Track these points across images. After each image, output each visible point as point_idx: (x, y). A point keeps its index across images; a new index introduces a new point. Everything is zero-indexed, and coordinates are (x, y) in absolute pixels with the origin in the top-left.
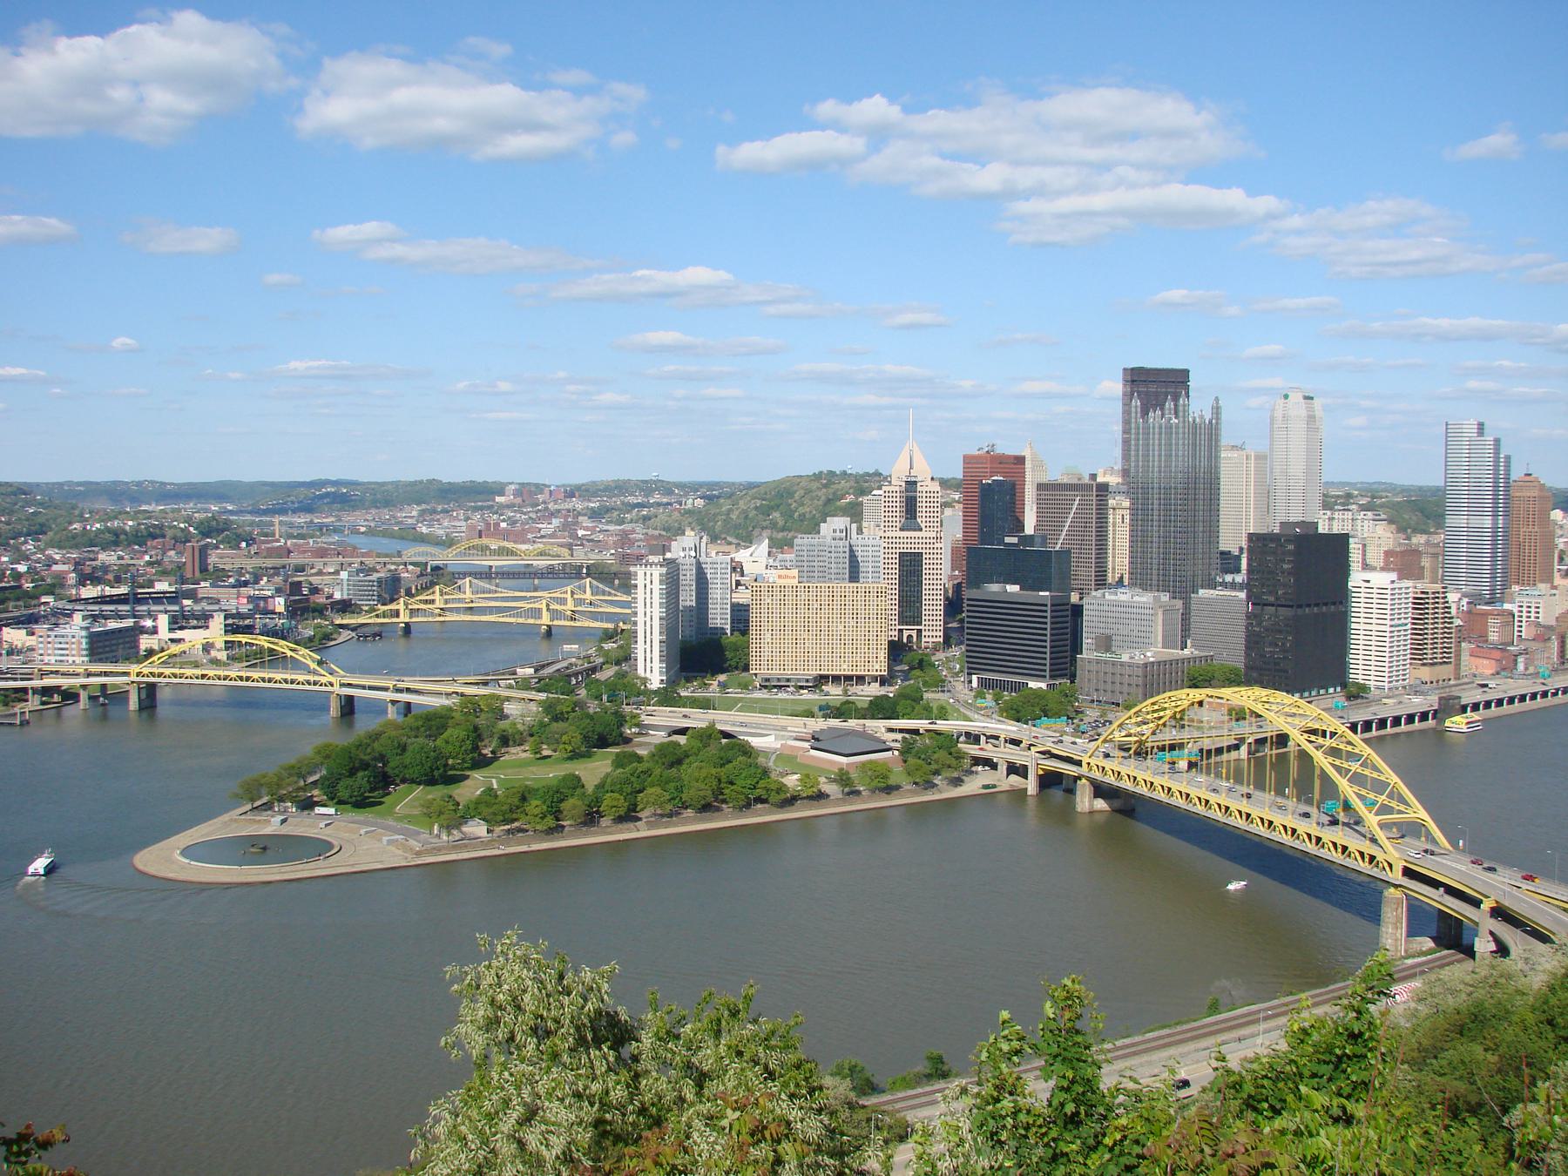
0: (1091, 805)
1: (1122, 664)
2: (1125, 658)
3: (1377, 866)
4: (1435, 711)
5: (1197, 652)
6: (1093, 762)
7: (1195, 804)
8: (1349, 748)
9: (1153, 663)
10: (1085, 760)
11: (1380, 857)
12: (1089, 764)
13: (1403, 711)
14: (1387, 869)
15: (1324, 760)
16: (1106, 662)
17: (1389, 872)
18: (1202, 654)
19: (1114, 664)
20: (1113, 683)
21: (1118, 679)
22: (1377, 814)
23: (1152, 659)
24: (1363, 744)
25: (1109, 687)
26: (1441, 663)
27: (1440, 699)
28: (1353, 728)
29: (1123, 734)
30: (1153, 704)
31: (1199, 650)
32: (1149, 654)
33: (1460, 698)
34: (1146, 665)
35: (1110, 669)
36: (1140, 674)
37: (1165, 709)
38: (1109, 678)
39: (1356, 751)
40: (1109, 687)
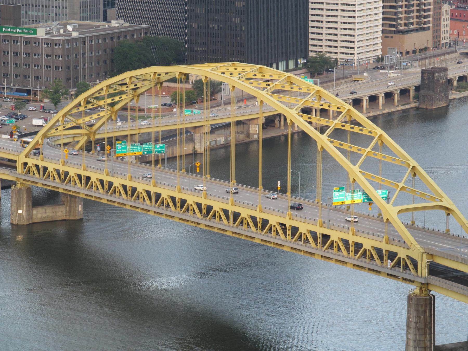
0: (30, 215)
1: (37, 41)
2: (41, 33)
3: (398, 264)
4: (417, 88)
5: (127, 24)
6: (31, 162)
7: (168, 206)
8: (357, 129)
9: (76, 39)
10: (21, 159)
11: (402, 253)
12: (25, 164)
13: (380, 91)
14: (411, 267)
15: (331, 145)
16: (16, 40)
17: (413, 272)
18: (137, 26)
19: (27, 41)
20: (26, 65)
21: (32, 59)
22: (394, 205)
23: (75, 34)
24: (371, 123)
25: (21, 70)
26: (417, 30)
27: (423, 72)
28: (357, 103)
29: (69, 126)
30: (109, 87)
31: (131, 22)
32: (70, 28)
33: (446, 70)
34: (68, 42)
35: (21, 48)
36: (61, 53)
37: (121, 93)
38: (21, 60)
39: (365, 132)
40: (21, 70)
